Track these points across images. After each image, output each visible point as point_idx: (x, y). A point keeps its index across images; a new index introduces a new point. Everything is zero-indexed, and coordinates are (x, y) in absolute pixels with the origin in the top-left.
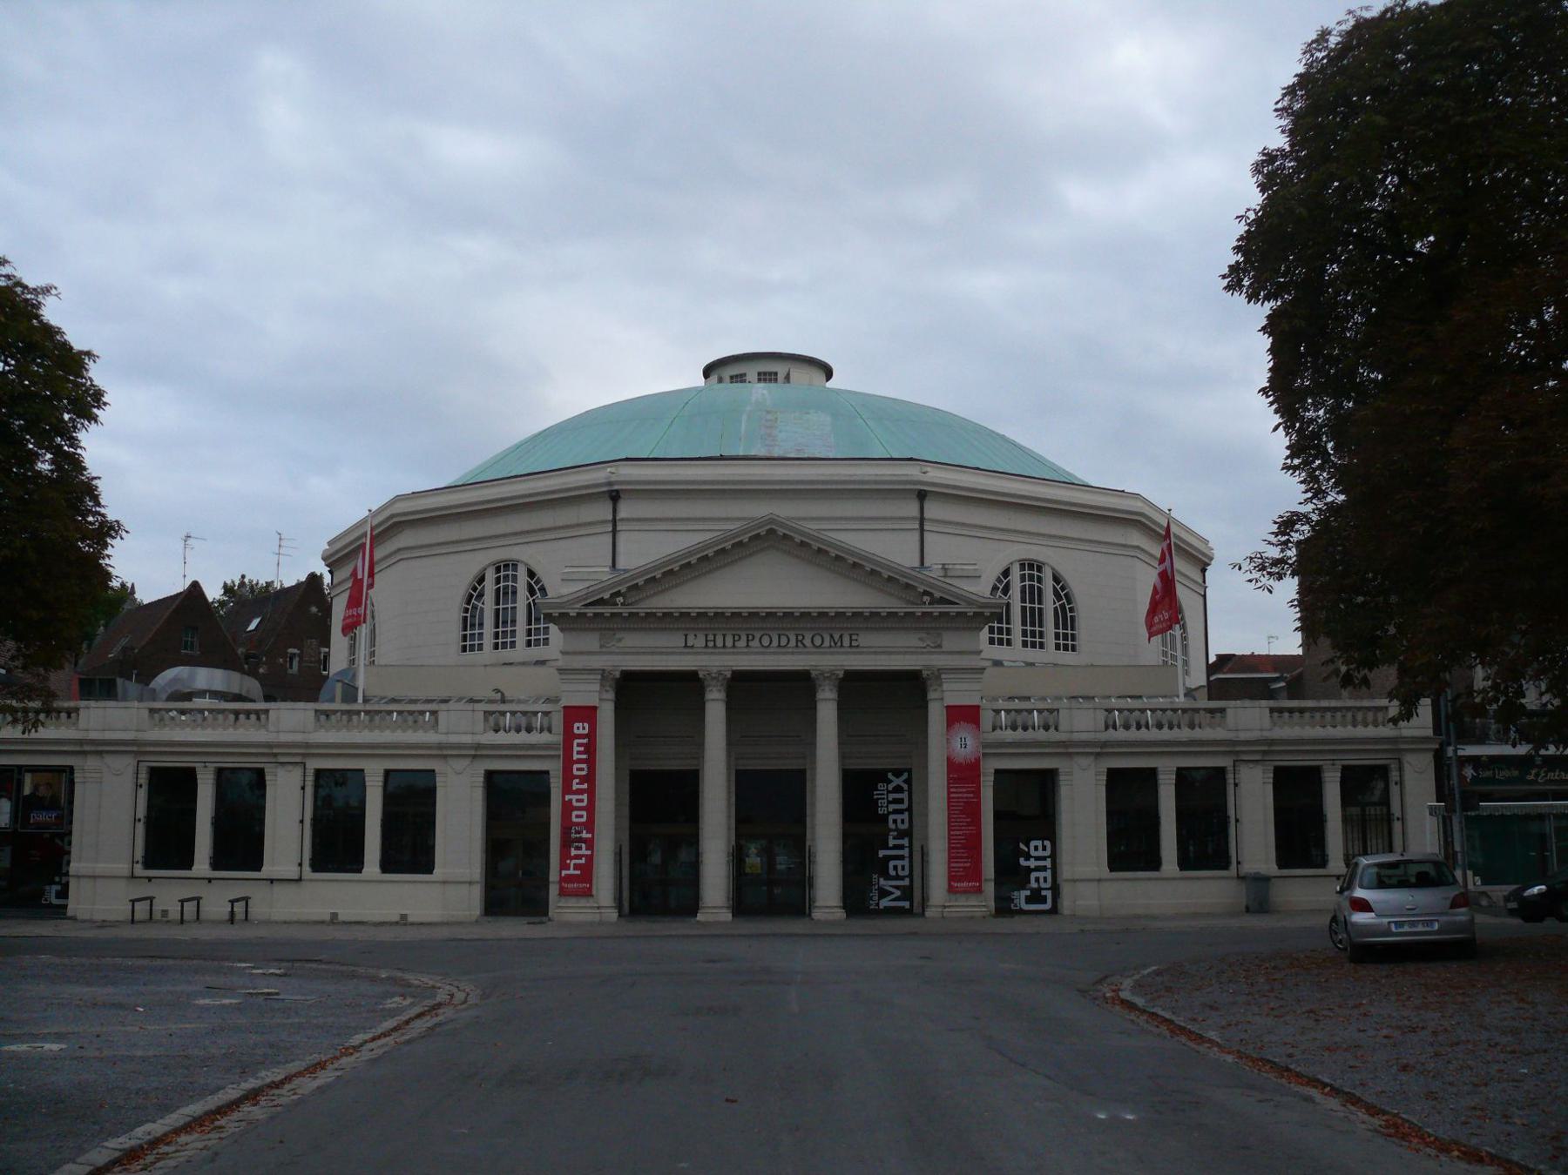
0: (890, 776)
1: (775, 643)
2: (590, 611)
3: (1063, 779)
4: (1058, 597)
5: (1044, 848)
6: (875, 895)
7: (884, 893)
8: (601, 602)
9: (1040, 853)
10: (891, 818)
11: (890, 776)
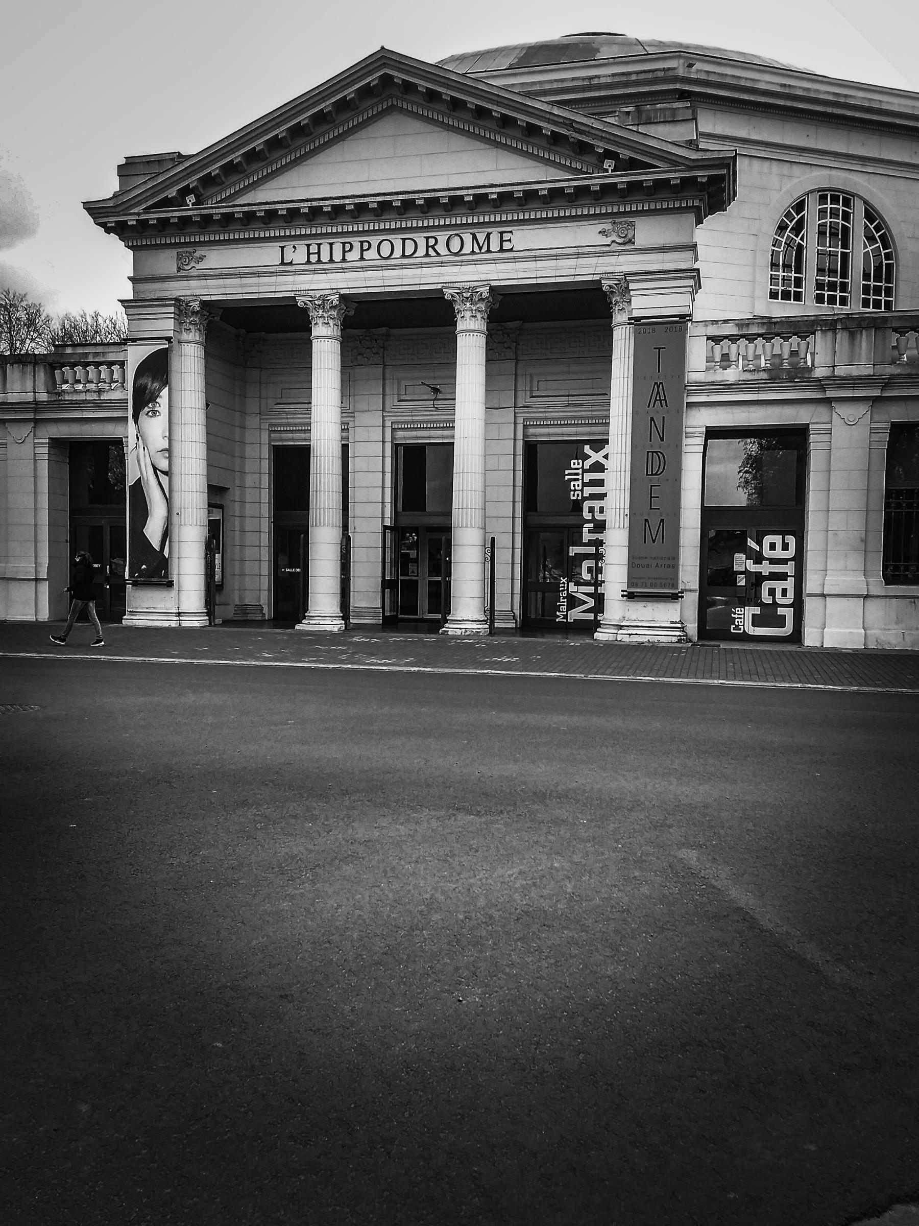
0: (587, 449)
1: (398, 253)
2: (153, 217)
3: (815, 441)
4: (871, 239)
5: (785, 547)
6: (563, 603)
7: (573, 602)
8: (166, 203)
9: (779, 553)
10: (586, 505)
11: (587, 449)
